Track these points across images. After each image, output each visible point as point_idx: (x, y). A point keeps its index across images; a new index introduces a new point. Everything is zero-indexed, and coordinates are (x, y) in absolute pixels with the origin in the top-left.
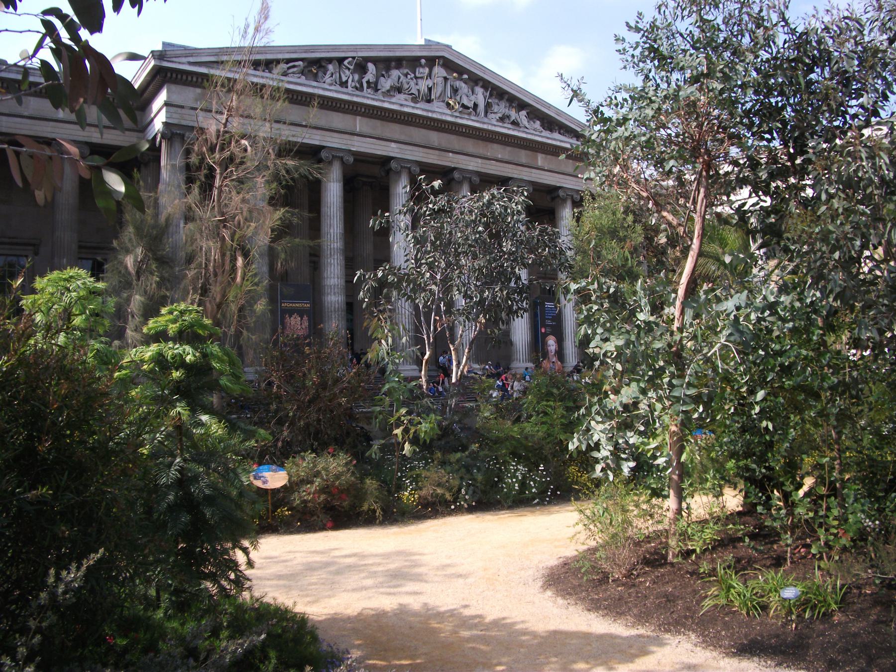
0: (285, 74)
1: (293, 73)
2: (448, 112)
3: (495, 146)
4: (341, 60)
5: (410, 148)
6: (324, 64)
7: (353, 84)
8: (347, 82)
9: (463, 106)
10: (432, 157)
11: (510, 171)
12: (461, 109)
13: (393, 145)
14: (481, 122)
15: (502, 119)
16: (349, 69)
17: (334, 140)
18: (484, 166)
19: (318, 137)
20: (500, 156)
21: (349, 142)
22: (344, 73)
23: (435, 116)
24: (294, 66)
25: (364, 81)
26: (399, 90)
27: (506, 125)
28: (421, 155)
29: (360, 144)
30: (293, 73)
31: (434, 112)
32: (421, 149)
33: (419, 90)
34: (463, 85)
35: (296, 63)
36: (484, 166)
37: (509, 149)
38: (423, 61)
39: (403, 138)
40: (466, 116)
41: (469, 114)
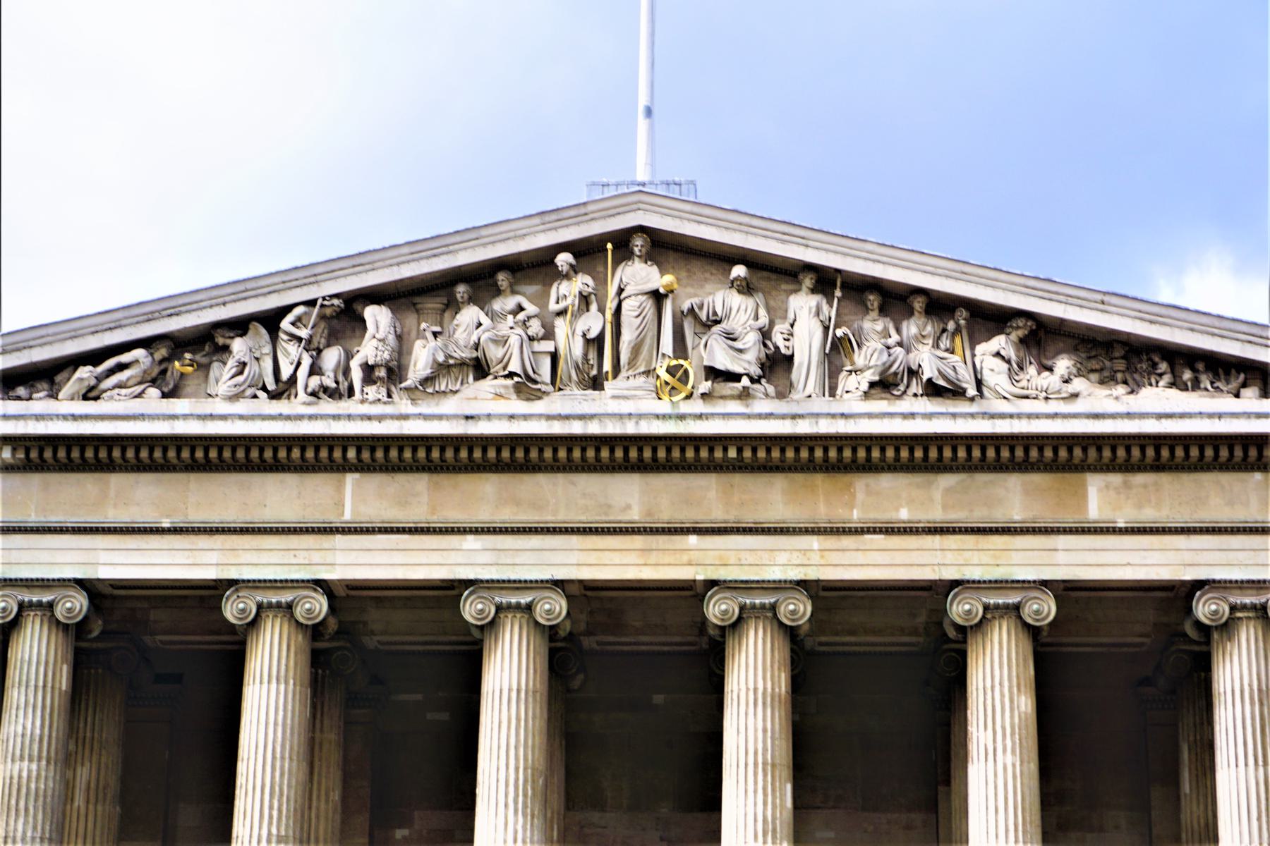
0: (90, 394)
1: (120, 386)
2: (664, 406)
3: (886, 482)
4: (271, 320)
6: (221, 341)
7: (315, 382)
8: (293, 380)
9: (713, 373)
10: (616, 558)
11: (950, 557)
12: (705, 386)
13: (471, 541)
14: (783, 417)
15: (885, 385)
16: (300, 339)
17: (265, 558)
19: (213, 557)
21: (316, 557)
22: (287, 353)
23: (594, 428)
24: (122, 367)
25: (355, 365)
26: (480, 369)
27: (906, 405)
28: (574, 558)
29: (352, 557)
30: (120, 386)
31: (592, 417)
32: (575, 540)
33: (555, 357)
34: (736, 300)
35: (125, 358)
36: (835, 558)
37: (947, 481)
38: (564, 259)
39: (507, 516)
40: (734, 407)
41: (745, 395)
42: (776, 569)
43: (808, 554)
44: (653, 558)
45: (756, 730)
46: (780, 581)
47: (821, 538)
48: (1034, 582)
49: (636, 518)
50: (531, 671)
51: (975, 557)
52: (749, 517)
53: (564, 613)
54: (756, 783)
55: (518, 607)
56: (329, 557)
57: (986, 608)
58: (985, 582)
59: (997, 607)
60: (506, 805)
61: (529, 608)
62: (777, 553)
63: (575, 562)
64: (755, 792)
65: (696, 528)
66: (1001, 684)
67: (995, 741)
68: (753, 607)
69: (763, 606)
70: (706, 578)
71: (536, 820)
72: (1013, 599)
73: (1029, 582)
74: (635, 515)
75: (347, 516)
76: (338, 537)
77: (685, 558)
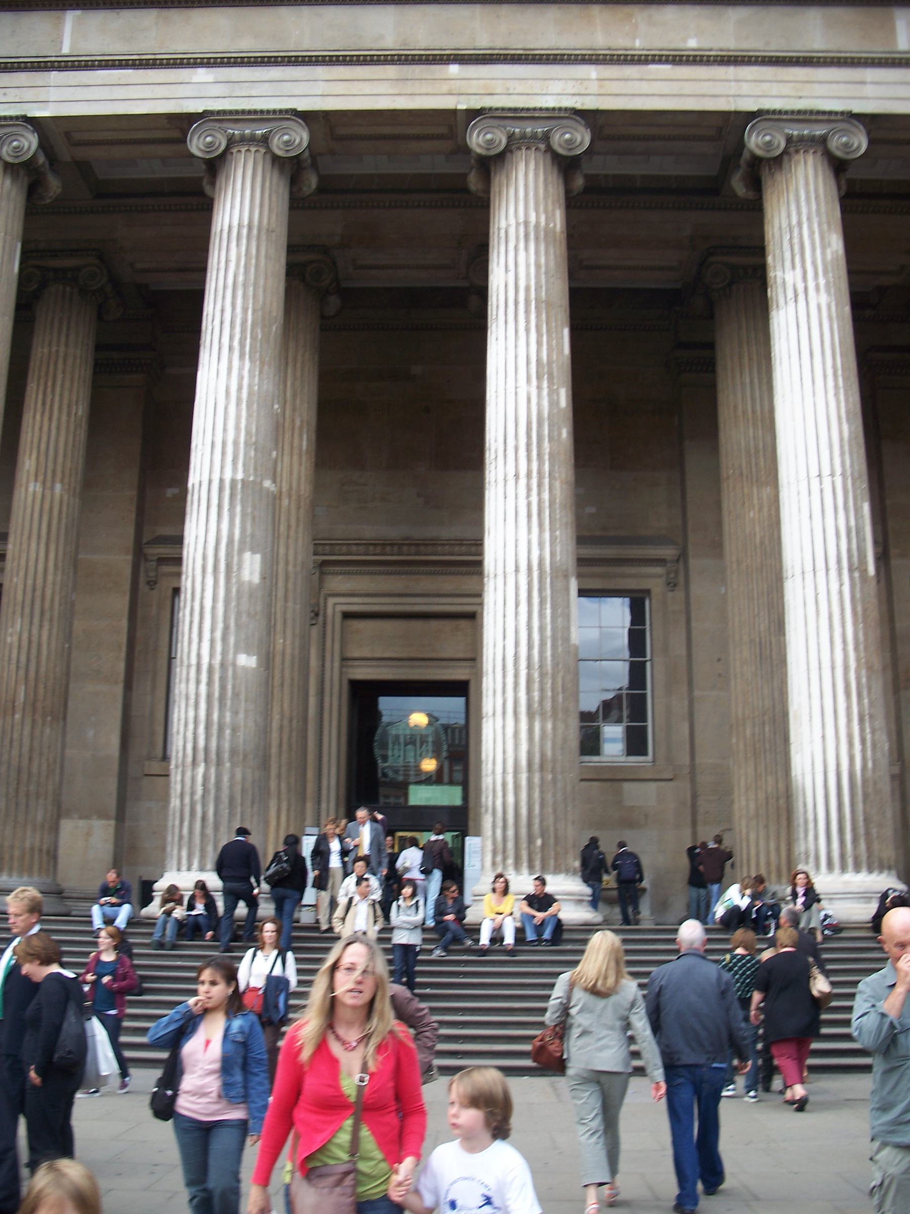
5: (275, 72)
10: (367, 88)
11: (745, 88)
13: (202, 75)
18: (615, 87)
20: (692, 43)
21: (29, 95)
28: (321, 88)
32: (321, 71)
36: (615, 87)
39: (246, 45)
42: (549, 98)
43: (586, 83)
44: (409, 88)
45: (528, 266)
46: (554, 109)
47: (600, 67)
48: (842, 113)
49: (390, 46)
50: (266, 208)
51: (775, 89)
52: (517, 44)
53: (305, 144)
54: (528, 321)
55: (252, 140)
56: (42, 95)
57: (789, 139)
58: (786, 112)
59: (801, 139)
60: (231, 348)
61: (265, 140)
62: (551, 82)
63: (320, 93)
64: (527, 330)
65: (458, 55)
66: (809, 219)
67: (805, 279)
68: (523, 136)
69: (534, 136)
70: (469, 108)
71: (266, 367)
72: (819, 131)
73: (836, 113)
74: (390, 42)
75: (66, 50)
76: (55, 77)
77: (445, 88)
